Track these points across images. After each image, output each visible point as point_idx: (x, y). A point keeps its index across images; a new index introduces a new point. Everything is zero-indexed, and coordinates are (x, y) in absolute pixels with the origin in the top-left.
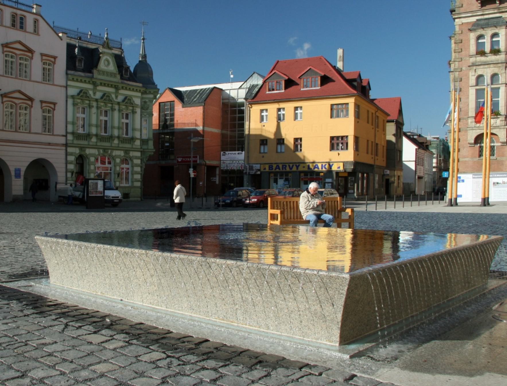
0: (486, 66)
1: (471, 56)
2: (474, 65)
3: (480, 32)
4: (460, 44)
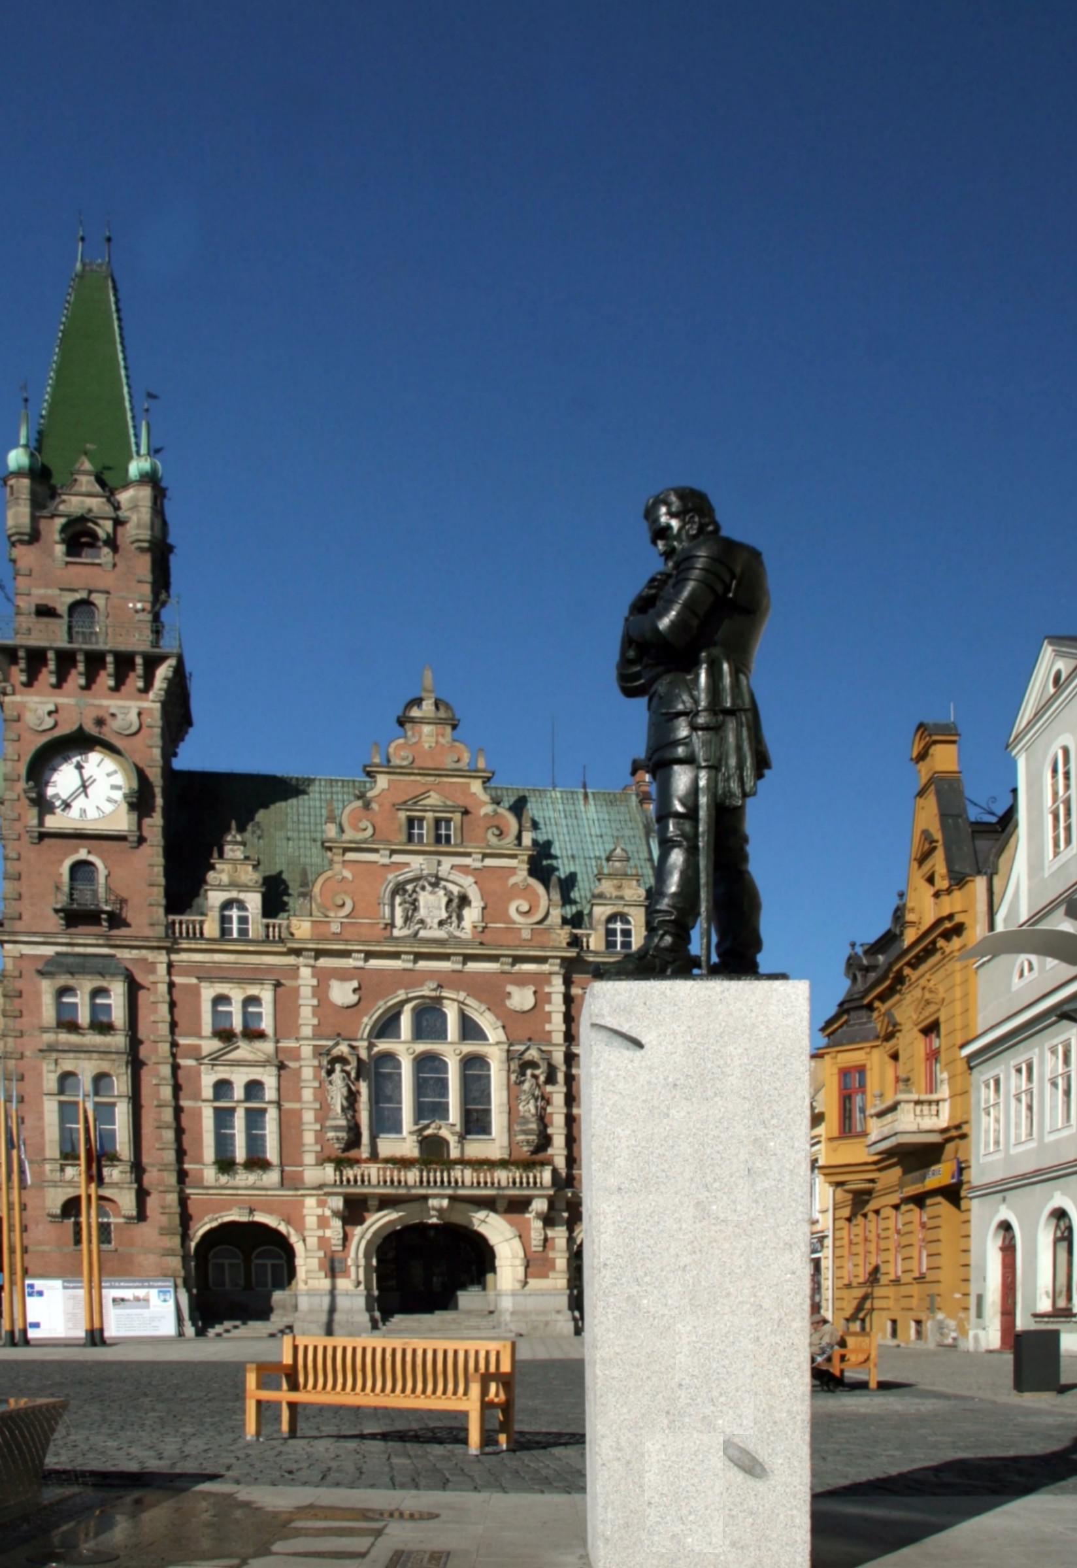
0: (82, 1055)
1: (45, 1030)
2: (51, 1049)
3: (63, 980)
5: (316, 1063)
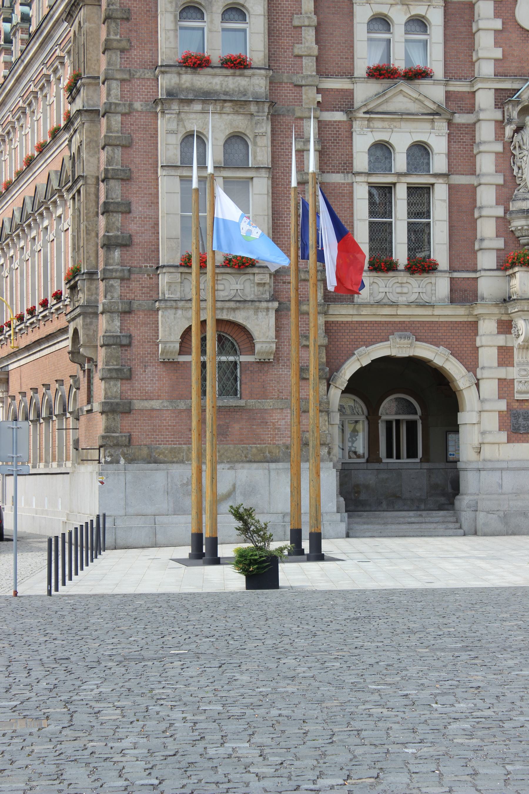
1: (166, 68)
4: (126, 25)
5: (498, 115)
